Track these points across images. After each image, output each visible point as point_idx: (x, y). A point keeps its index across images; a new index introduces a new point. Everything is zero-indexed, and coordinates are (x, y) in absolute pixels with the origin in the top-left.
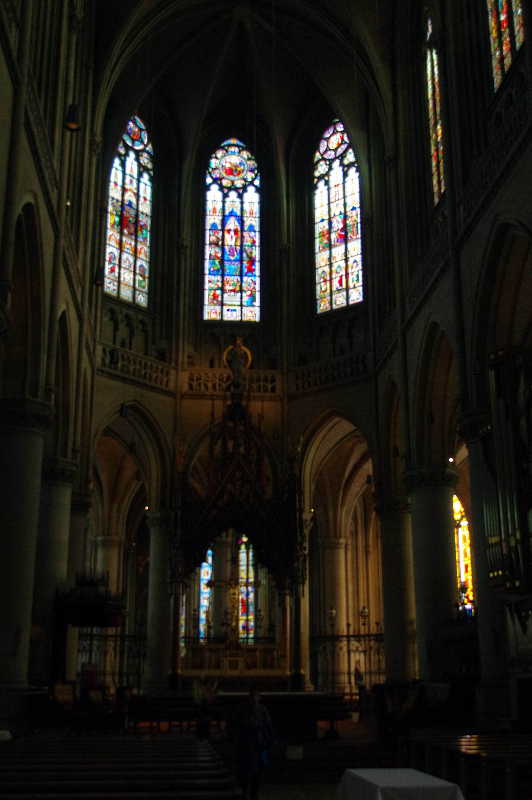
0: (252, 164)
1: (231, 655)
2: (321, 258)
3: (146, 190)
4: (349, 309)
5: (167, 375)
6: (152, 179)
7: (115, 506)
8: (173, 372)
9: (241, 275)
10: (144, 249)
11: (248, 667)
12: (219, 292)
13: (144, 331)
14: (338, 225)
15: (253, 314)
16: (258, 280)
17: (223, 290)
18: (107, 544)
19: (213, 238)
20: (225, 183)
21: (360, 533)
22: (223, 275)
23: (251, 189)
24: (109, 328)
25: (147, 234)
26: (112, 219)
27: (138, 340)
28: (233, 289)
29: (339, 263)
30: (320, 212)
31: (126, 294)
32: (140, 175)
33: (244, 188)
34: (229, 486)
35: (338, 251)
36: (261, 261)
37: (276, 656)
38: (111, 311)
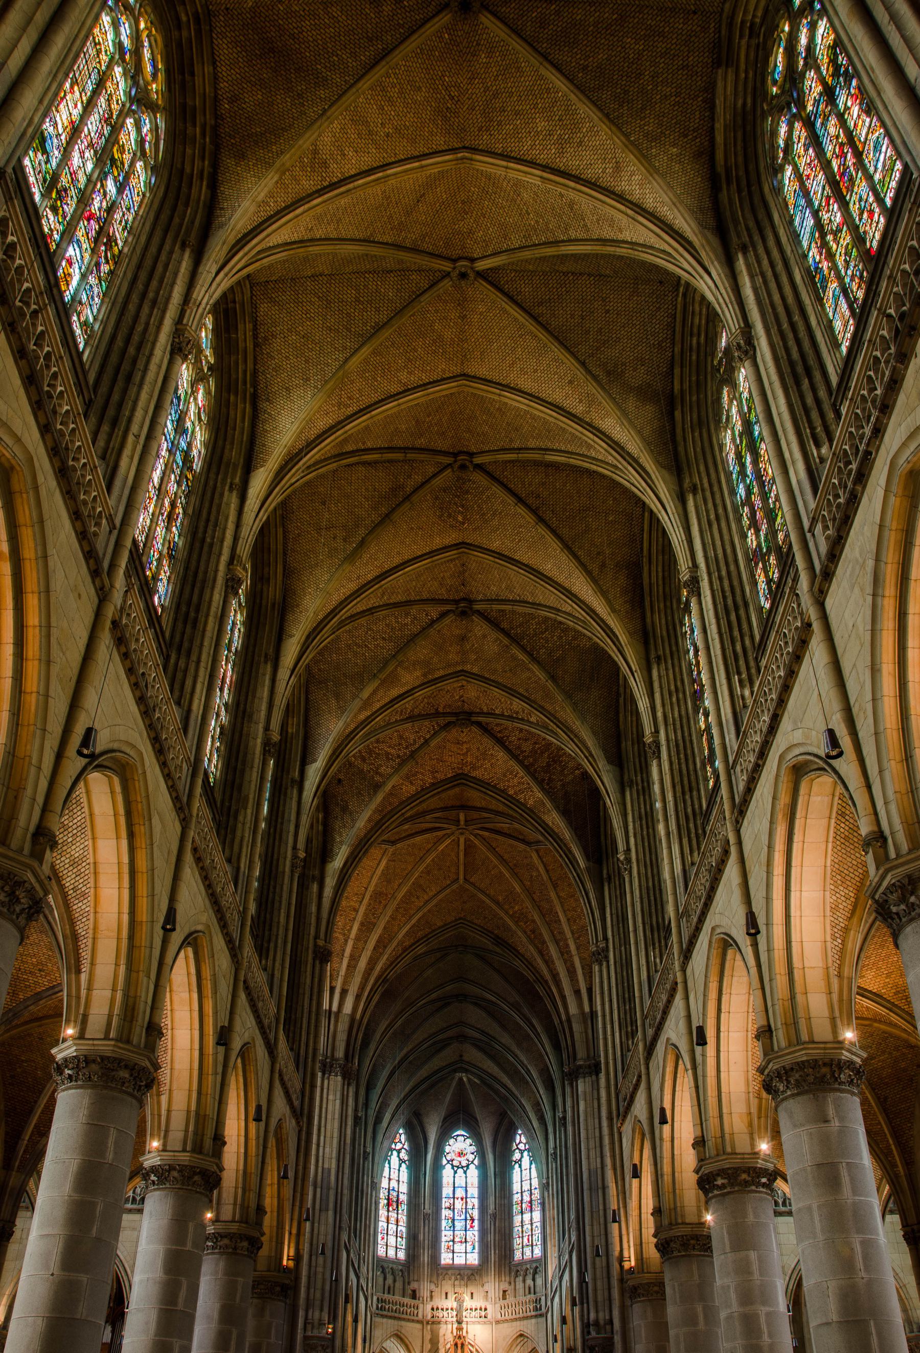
0: (473, 1149)
2: (517, 1219)
3: (404, 1175)
4: (532, 1261)
6: (408, 1168)
8: (421, 1306)
10: (403, 1218)
14: (526, 1198)
15: (474, 1259)
16: (476, 1233)
17: (453, 1241)
19: (447, 1205)
20: (455, 1163)
23: (472, 1167)
24: (381, 1280)
25: (404, 1207)
26: (383, 1202)
27: (399, 1285)
29: (527, 1227)
30: (516, 1187)
31: (391, 1253)
32: (400, 1166)
33: (468, 1166)
35: (527, 1217)
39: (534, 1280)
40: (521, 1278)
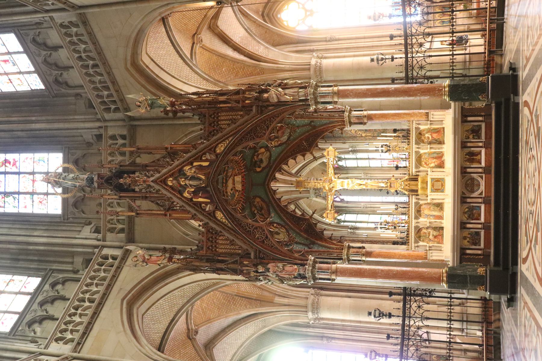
1: (425, 189)
5: (106, 258)
7: (277, 300)
8: (105, 251)
9: (19, 173)
11: (441, 165)
12: (35, 196)
13: (64, 282)
16: (24, 156)
17: (32, 194)
18: (316, 308)
21: (312, 48)
22: (19, 193)
28: (32, 182)
31: (20, 303)
34: (186, 194)
36: (6, 152)
37: (426, 127)
38: (30, 324)
39: (56, 48)
40: (65, 74)
